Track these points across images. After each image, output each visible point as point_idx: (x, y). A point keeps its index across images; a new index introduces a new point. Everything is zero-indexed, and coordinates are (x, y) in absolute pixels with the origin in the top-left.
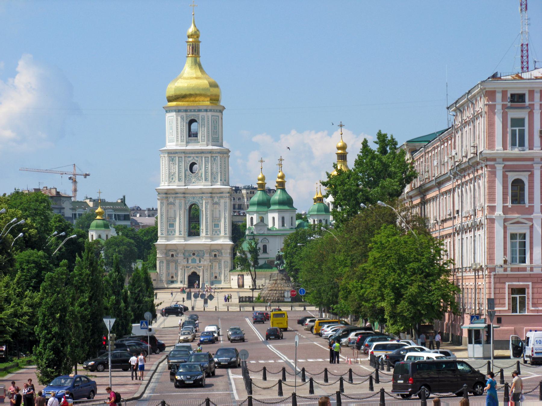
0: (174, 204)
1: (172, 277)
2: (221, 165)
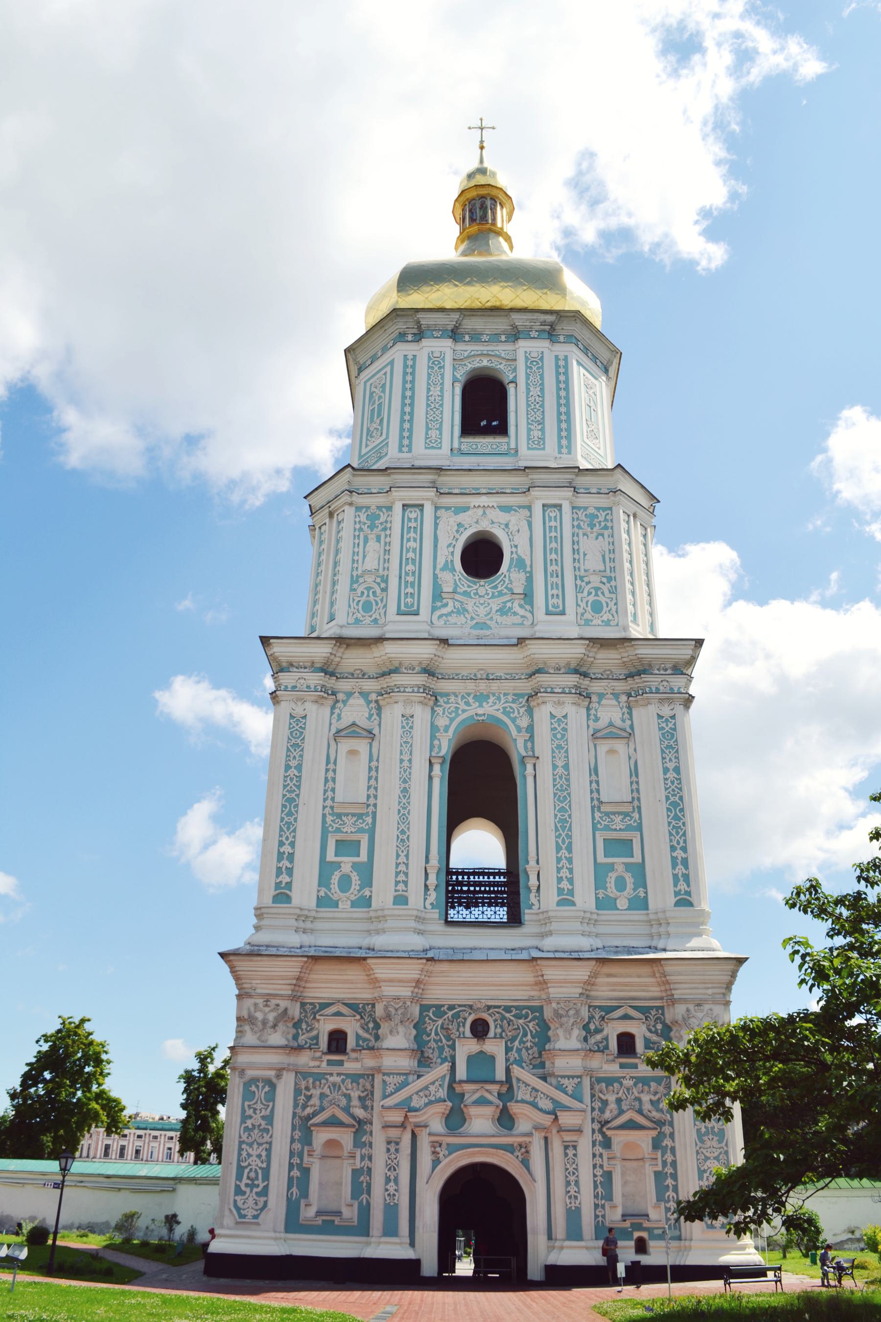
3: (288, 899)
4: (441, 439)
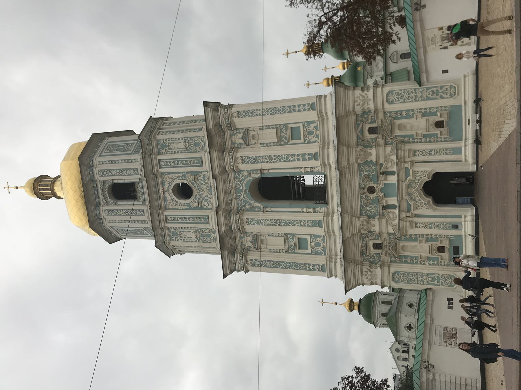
1: (441, 249)
2: (174, 132)
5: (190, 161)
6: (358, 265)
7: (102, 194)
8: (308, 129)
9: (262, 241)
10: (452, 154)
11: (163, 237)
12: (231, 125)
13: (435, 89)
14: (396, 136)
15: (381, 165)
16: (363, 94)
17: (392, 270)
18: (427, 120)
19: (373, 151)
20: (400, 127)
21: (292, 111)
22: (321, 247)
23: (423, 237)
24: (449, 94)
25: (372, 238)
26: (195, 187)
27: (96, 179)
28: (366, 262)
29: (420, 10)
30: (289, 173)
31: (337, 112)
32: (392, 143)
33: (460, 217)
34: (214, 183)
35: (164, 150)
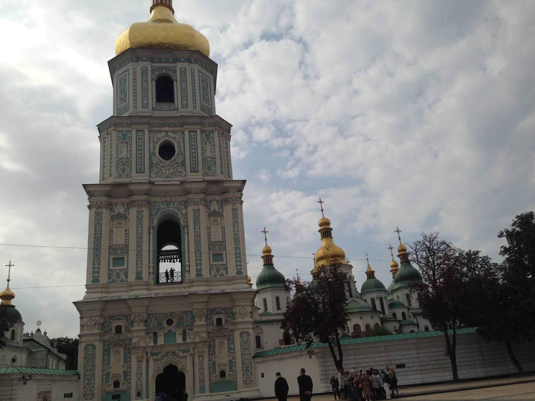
0: (125, 218)
1: (117, 384)
2: (220, 147)
3: (98, 281)
4: (148, 104)
5: (195, 161)
6: (101, 313)
7: (164, 67)
8: (221, 268)
9: (120, 223)
10: (200, 386)
11: (121, 124)
12: (226, 201)
13: (250, 369)
14: (214, 340)
15: (192, 330)
16: (248, 313)
17: (97, 344)
18: (226, 364)
19: (203, 322)
20: (222, 343)
21: (237, 256)
22: (116, 278)
23: (128, 368)
24: (246, 379)
25: (126, 325)
26: (171, 162)
27: (178, 64)
28: (103, 320)
29: (309, 355)
30: (185, 250)
31: (236, 293)
32: (209, 337)
33: (147, 397)
34: (175, 181)
35: (205, 137)
